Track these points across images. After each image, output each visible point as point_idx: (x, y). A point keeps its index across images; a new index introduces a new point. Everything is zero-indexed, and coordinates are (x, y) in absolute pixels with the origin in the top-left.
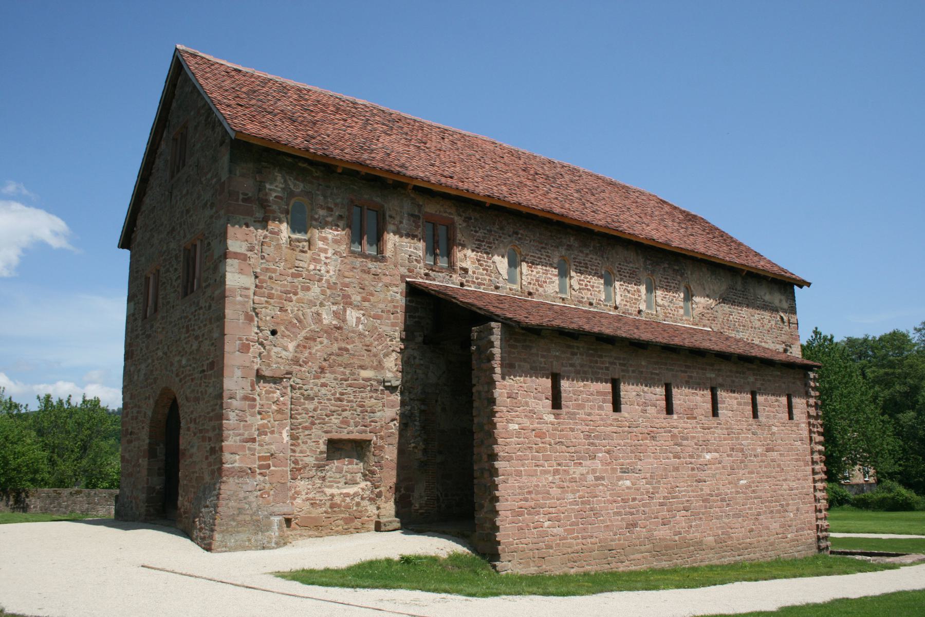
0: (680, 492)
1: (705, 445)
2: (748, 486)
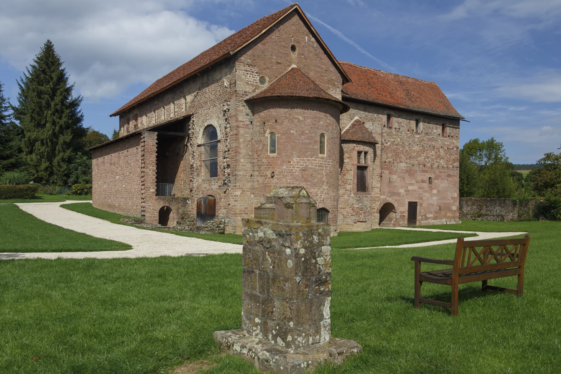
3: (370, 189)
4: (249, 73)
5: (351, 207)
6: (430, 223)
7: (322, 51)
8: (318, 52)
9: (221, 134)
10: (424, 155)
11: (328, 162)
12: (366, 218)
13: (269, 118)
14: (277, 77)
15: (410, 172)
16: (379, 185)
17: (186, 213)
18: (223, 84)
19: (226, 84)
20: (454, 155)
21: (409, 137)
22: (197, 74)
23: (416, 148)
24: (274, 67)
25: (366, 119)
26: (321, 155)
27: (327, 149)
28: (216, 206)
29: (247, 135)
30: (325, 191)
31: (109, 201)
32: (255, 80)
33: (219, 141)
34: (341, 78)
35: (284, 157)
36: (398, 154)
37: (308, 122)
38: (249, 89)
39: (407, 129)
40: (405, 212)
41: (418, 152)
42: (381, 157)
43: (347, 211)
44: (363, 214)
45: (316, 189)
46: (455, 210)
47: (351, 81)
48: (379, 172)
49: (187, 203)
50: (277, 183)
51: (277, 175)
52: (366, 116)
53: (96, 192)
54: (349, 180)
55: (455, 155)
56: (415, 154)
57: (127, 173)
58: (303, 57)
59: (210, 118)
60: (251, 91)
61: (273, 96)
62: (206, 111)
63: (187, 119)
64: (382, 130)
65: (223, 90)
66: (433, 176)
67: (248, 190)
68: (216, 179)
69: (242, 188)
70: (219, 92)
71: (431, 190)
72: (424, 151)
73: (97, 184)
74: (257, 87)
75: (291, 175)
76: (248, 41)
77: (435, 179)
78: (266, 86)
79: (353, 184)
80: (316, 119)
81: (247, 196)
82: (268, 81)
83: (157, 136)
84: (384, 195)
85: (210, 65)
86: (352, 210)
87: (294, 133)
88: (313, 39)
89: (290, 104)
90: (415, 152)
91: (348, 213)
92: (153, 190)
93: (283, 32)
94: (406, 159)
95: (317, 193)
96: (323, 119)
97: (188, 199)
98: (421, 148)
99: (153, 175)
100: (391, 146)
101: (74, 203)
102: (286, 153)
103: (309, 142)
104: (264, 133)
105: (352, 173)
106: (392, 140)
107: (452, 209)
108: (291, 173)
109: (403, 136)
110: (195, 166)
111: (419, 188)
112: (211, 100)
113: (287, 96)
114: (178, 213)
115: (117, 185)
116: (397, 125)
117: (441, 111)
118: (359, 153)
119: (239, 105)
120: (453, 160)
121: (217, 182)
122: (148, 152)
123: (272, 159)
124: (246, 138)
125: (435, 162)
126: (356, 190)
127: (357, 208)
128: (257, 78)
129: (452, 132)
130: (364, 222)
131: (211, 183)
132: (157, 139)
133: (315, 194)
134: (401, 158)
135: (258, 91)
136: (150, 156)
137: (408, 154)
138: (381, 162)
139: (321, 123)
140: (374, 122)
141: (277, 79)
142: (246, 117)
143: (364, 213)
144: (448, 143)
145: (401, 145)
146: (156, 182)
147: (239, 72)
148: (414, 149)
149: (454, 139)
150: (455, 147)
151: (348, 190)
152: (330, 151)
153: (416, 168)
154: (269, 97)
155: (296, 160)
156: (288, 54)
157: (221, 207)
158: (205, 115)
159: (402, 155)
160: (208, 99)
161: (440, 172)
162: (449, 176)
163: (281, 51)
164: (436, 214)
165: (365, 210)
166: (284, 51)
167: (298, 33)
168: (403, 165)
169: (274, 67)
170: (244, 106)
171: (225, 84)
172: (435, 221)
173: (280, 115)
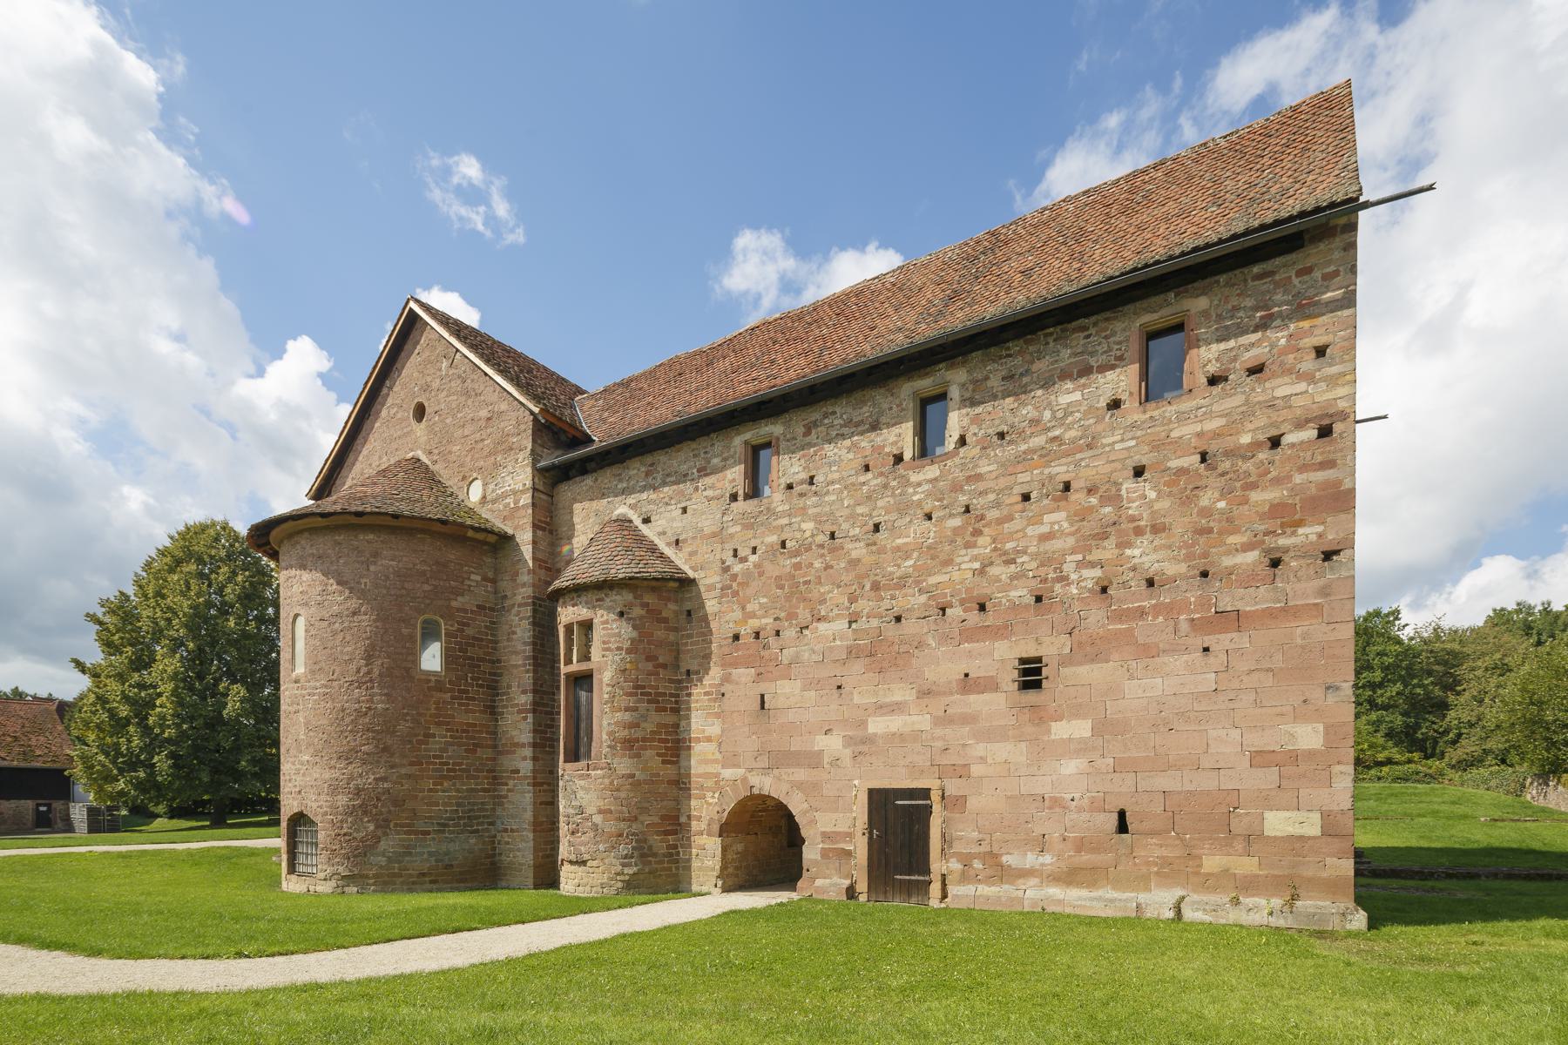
36: (802, 588)
90: (908, 557)
94: (853, 599)
111: (945, 720)
137: (860, 577)
148: (899, 541)
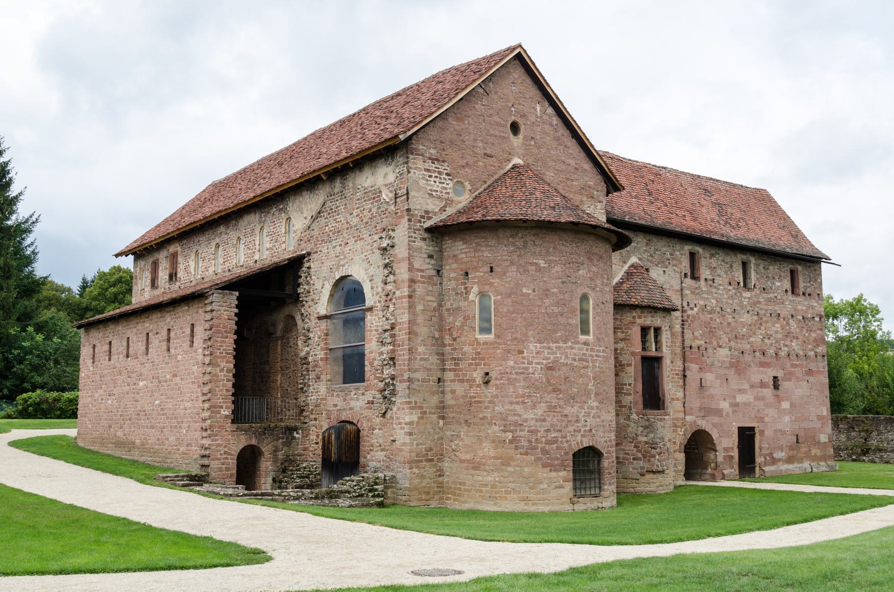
0: (128, 408)
1: (140, 377)
2: (160, 405)
3: (667, 404)
4: (434, 175)
5: (632, 442)
6: (781, 470)
7: (567, 133)
8: (560, 134)
9: (373, 295)
10: (761, 331)
11: (597, 351)
12: (664, 463)
13: (478, 263)
14: (485, 182)
15: (737, 366)
16: (680, 394)
17: (290, 459)
18: (379, 196)
19: (387, 195)
20: (815, 331)
21: (731, 297)
22: (322, 175)
23: (746, 318)
24: (480, 163)
25: (651, 262)
26: (583, 338)
27: (593, 326)
28: (361, 444)
29: (430, 298)
30: (594, 411)
31: (120, 434)
32: (446, 188)
33: (370, 309)
34: (603, 183)
35: (509, 343)
37: (557, 272)
38: (433, 206)
39: (727, 280)
40: (732, 448)
41: (750, 325)
42: (683, 336)
43: (624, 450)
44: (657, 457)
45: (576, 408)
46: (825, 443)
47: (624, 189)
48: (679, 367)
49: (294, 438)
50: (497, 395)
51: (496, 379)
52: (651, 256)
53: (86, 413)
54: (626, 384)
55: (818, 332)
56: (745, 330)
57: (165, 376)
58: (533, 143)
59: (347, 263)
60: (437, 210)
61: (487, 220)
62: (338, 248)
63: (296, 264)
64: (682, 283)
65: (379, 208)
66: (780, 374)
67: (433, 411)
68: (362, 389)
69: (421, 408)
70: (369, 212)
71: (779, 402)
72: (761, 324)
73: (92, 396)
74: (449, 202)
75: (524, 380)
76: (432, 113)
77: (784, 380)
78: (464, 200)
79: (635, 394)
80: (572, 265)
81: (432, 423)
82: (470, 190)
83: (238, 299)
84: (692, 414)
85: (351, 160)
86: (635, 447)
87: (530, 294)
88: (550, 110)
89: (520, 235)
90: (744, 327)
91: (628, 454)
92: (226, 413)
93: (495, 97)
94: (730, 341)
95: (577, 416)
96: (585, 266)
97: (295, 429)
98: (756, 318)
99: (228, 380)
100: (700, 314)
101: (35, 435)
102: (513, 333)
103: (559, 312)
104: (466, 294)
105: (631, 370)
106: (702, 303)
107: (819, 440)
108: (526, 376)
109: (721, 294)
110: (310, 359)
111: (757, 398)
112: (351, 228)
113: (516, 220)
114: (275, 460)
115: (140, 400)
116: (708, 272)
117: (785, 244)
118: (644, 330)
119: (415, 238)
120: (815, 340)
121: (363, 394)
122: (219, 332)
123: (485, 347)
124: (429, 303)
125: (782, 345)
126: (641, 406)
127: (646, 443)
128: (447, 184)
129: (809, 285)
130: (659, 472)
131: (350, 395)
132: (237, 307)
133: (574, 419)
134: (720, 339)
135: (450, 211)
136: (222, 342)
137: (732, 331)
138: (684, 348)
139: (581, 272)
140: (667, 268)
141: (486, 186)
142: (428, 260)
143: (659, 454)
144: (804, 308)
145: (719, 313)
146: (233, 395)
147: (415, 173)
148: (742, 320)
149: (814, 299)
150: (817, 315)
151: (625, 407)
152: (600, 328)
153: (748, 358)
154: (477, 221)
155: (534, 349)
156: (504, 138)
157: (372, 446)
158: (336, 257)
159: (721, 333)
160: (342, 224)
161: (793, 366)
162: (810, 372)
163: (492, 132)
164: (791, 452)
165: (660, 448)
166: (497, 133)
167: (523, 99)
168: (723, 352)
169: (480, 163)
170: (424, 239)
171: (384, 196)
172: (790, 467)
173: (500, 258)
